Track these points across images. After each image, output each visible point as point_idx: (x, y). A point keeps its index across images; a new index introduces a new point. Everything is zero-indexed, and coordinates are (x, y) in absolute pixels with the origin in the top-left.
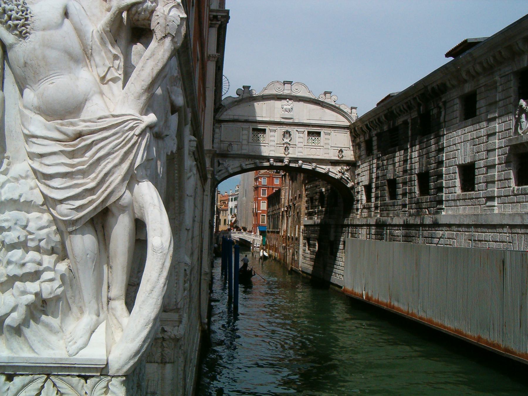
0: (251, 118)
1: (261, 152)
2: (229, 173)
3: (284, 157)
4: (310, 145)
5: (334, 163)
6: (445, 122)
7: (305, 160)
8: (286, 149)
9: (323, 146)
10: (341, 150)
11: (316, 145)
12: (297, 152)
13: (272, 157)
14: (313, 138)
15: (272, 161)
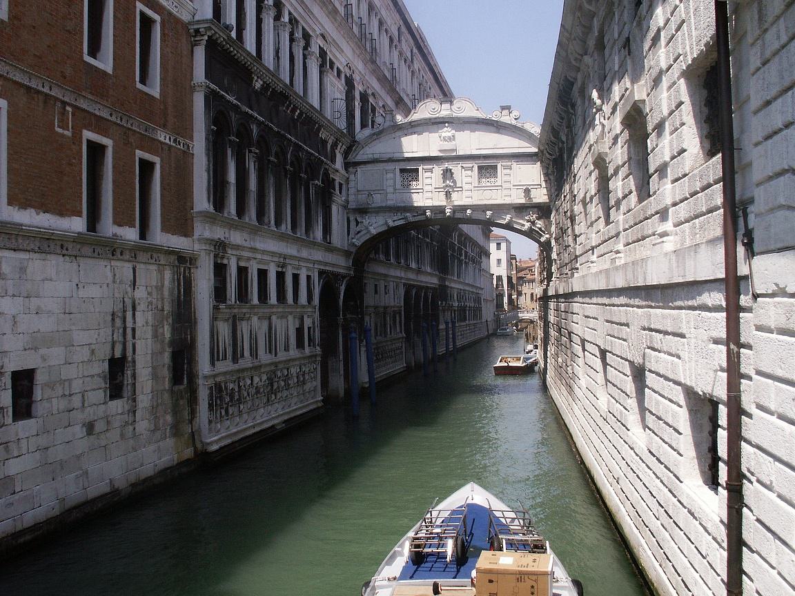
0: (397, 156)
1: (412, 202)
2: (371, 234)
3: (446, 206)
4: (484, 185)
5: (520, 209)
6: (576, 135)
7: (475, 208)
8: (448, 195)
9: (502, 186)
10: (527, 188)
11: (493, 185)
12: (464, 197)
13: (428, 208)
14: (488, 175)
15: (428, 213)
